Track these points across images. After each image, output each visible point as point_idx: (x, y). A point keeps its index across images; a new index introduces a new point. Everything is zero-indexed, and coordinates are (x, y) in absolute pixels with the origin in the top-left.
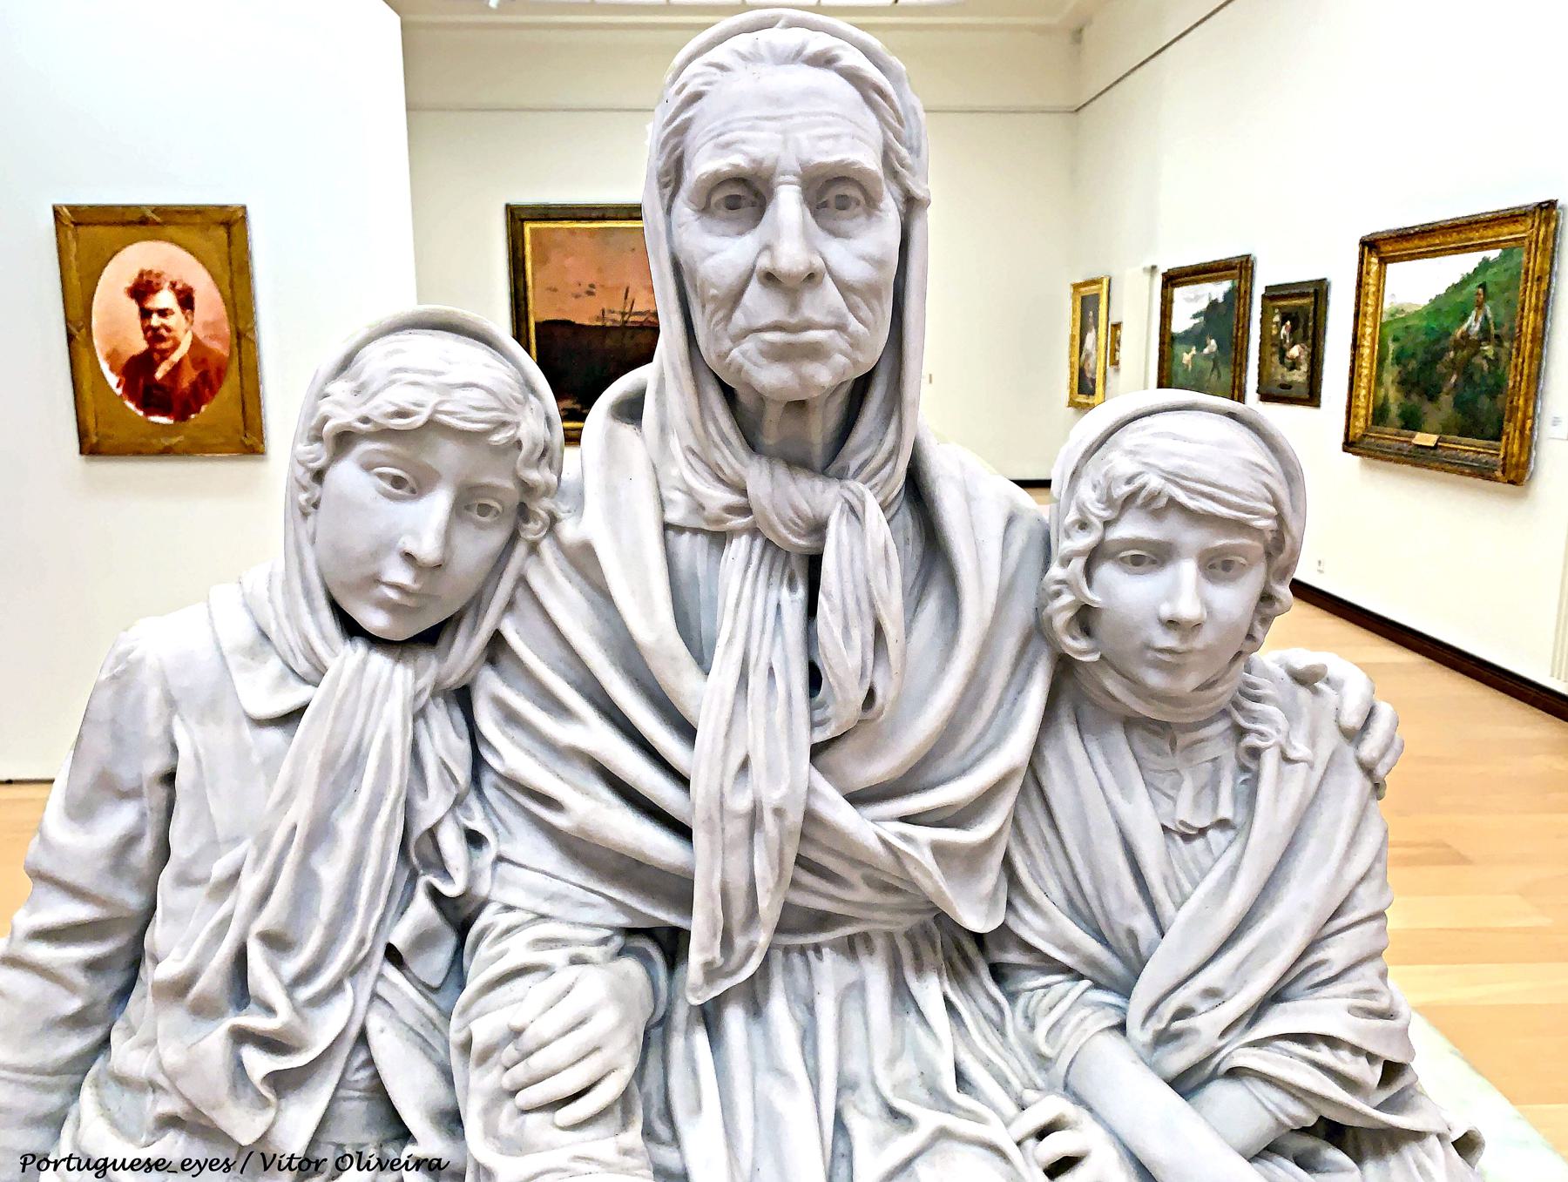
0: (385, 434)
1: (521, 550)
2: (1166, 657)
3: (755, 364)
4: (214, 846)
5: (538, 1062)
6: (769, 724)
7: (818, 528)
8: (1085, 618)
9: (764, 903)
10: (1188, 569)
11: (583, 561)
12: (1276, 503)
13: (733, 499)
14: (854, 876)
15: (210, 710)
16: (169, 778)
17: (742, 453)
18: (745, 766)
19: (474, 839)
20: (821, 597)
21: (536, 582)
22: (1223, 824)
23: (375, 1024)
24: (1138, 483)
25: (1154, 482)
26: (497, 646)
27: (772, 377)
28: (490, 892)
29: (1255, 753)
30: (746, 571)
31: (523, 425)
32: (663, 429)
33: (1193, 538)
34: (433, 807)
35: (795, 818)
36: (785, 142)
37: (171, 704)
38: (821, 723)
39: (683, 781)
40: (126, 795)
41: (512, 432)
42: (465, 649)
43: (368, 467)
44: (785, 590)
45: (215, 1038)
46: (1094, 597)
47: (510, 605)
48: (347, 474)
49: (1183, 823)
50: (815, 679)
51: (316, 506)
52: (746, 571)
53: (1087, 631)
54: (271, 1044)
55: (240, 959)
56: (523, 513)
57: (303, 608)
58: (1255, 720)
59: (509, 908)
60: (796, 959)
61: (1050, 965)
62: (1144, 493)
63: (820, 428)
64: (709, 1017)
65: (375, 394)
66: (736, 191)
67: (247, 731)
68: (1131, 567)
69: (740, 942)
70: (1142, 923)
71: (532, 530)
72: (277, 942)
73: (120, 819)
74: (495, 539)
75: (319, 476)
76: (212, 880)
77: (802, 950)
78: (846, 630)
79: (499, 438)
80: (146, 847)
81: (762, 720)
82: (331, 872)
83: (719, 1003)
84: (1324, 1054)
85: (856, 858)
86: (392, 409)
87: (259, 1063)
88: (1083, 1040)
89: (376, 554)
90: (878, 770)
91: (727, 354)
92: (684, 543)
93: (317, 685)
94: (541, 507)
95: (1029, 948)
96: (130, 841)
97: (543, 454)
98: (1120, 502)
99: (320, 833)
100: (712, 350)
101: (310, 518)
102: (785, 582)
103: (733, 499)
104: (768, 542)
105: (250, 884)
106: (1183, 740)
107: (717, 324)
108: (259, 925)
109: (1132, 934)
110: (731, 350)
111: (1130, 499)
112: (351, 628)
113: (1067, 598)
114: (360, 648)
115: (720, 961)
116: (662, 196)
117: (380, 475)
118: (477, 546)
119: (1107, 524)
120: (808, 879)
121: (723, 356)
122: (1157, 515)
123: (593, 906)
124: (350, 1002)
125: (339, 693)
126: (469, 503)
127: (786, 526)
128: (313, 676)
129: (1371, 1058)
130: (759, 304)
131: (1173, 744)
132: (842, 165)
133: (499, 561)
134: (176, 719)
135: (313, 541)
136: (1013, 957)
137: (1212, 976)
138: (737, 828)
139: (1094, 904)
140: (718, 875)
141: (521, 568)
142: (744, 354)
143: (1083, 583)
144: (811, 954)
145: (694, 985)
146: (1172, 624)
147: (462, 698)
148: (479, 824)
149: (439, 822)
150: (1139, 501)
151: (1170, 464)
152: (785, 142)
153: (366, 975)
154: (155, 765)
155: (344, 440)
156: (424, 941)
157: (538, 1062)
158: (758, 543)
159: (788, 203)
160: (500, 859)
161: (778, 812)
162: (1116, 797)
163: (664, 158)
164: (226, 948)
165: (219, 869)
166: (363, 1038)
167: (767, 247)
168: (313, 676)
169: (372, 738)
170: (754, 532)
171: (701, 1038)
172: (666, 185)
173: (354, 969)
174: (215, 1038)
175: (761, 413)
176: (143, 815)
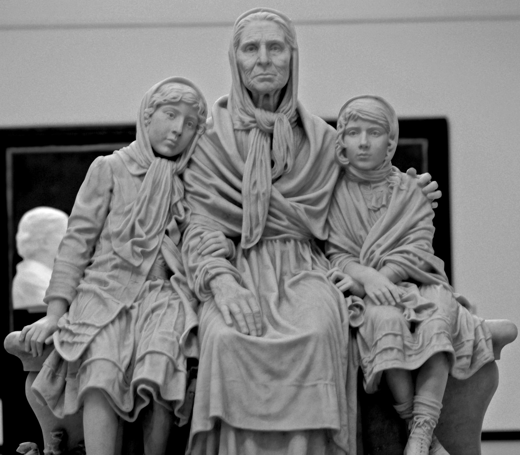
0: (170, 103)
1: (197, 137)
2: (362, 157)
3: (256, 83)
4: (124, 205)
5: (208, 243)
6: (261, 174)
7: (272, 124)
8: (344, 151)
9: (261, 219)
10: (364, 134)
11: (214, 139)
12: (385, 118)
13: (252, 119)
14: (284, 217)
15: (121, 175)
16: (111, 191)
17: (254, 108)
18: (255, 183)
19: (186, 210)
20: (273, 139)
21: (201, 144)
22: (383, 206)
23: (163, 248)
24: (351, 114)
25: (354, 112)
26: (190, 162)
27: (261, 86)
28: (190, 221)
29: (392, 188)
30: (255, 136)
31: (200, 104)
32: (233, 108)
33: (365, 126)
34: (176, 198)
35: (267, 196)
36: (262, 36)
37: (112, 172)
38: (274, 174)
39: (239, 191)
40: (99, 195)
41: (197, 105)
42: (182, 163)
43: (164, 112)
44: (265, 142)
45: (129, 243)
46: (345, 146)
47: (194, 152)
48: (160, 114)
49: (373, 207)
50: (273, 163)
51: (149, 123)
52: (255, 136)
53: (345, 156)
54: (141, 244)
55: (133, 228)
56: (198, 127)
57: (145, 149)
58: (391, 180)
59: (195, 224)
60: (269, 243)
61: (341, 250)
62: (352, 116)
63: (273, 101)
64: (246, 254)
65: (166, 95)
66: (252, 47)
67: (131, 179)
68: (352, 135)
69: (255, 232)
70: (362, 233)
71: (200, 132)
72: (142, 223)
73: (97, 202)
74: (191, 133)
75: (151, 116)
76: (124, 212)
77: (271, 241)
78: (279, 147)
79: (195, 106)
80: (103, 210)
81: (259, 173)
82: (154, 209)
83: (249, 250)
84: (405, 255)
85: (285, 212)
86: (172, 97)
87: (139, 250)
88: (347, 263)
89: (167, 131)
90: (289, 185)
91: (250, 82)
92: (239, 134)
93: (148, 169)
94: (202, 126)
95: (336, 247)
96: (99, 208)
97: (203, 112)
98: (347, 119)
99: (151, 200)
100: (246, 81)
101: (148, 127)
102: (265, 139)
103: (252, 119)
104: (261, 131)
105: (136, 209)
106: (373, 185)
107: (248, 75)
108: (139, 218)
109: (361, 237)
110: (251, 81)
111: (349, 118)
112: (157, 154)
113: (339, 147)
114: (158, 159)
115: (249, 237)
116: (234, 49)
117: (168, 114)
118: (188, 133)
119: (346, 125)
120: (272, 218)
121: (249, 83)
122: (356, 120)
123: (217, 225)
124: (158, 240)
125: (156, 165)
126: (187, 121)
127: (265, 123)
128: (147, 166)
129: (420, 259)
130: (258, 70)
131: (370, 187)
132: (274, 41)
133: (193, 137)
134: (114, 176)
135: (148, 132)
136: (332, 250)
137: (379, 242)
138: (253, 198)
139: (351, 231)
140: (249, 211)
141: (197, 142)
142: (254, 82)
143: (342, 141)
144: (274, 242)
145: (243, 245)
146: (361, 147)
147: (181, 176)
148: (186, 205)
149: (177, 202)
150: (352, 117)
151: (358, 108)
152: (262, 36)
153: (161, 235)
154: (109, 186)
155: (159, 106)
156: (174, 231)
157: (208, 243)
158: (258, 130)
159: (263, 49)
160: (192, 214)
161: (264, 194)
162: (355, 201)
163: (235, 40)
164: (130, 224)
165: (127, 208)
166: (160, 252)
167: (259, 58)
168: (147, 166)
169: (163, 178)
170: (257, 127)
171: (245, 261)
172: (236, 46)
173: (158, 233)
174: (129, 243)
175: (258, 98)
176: (103, 201)
